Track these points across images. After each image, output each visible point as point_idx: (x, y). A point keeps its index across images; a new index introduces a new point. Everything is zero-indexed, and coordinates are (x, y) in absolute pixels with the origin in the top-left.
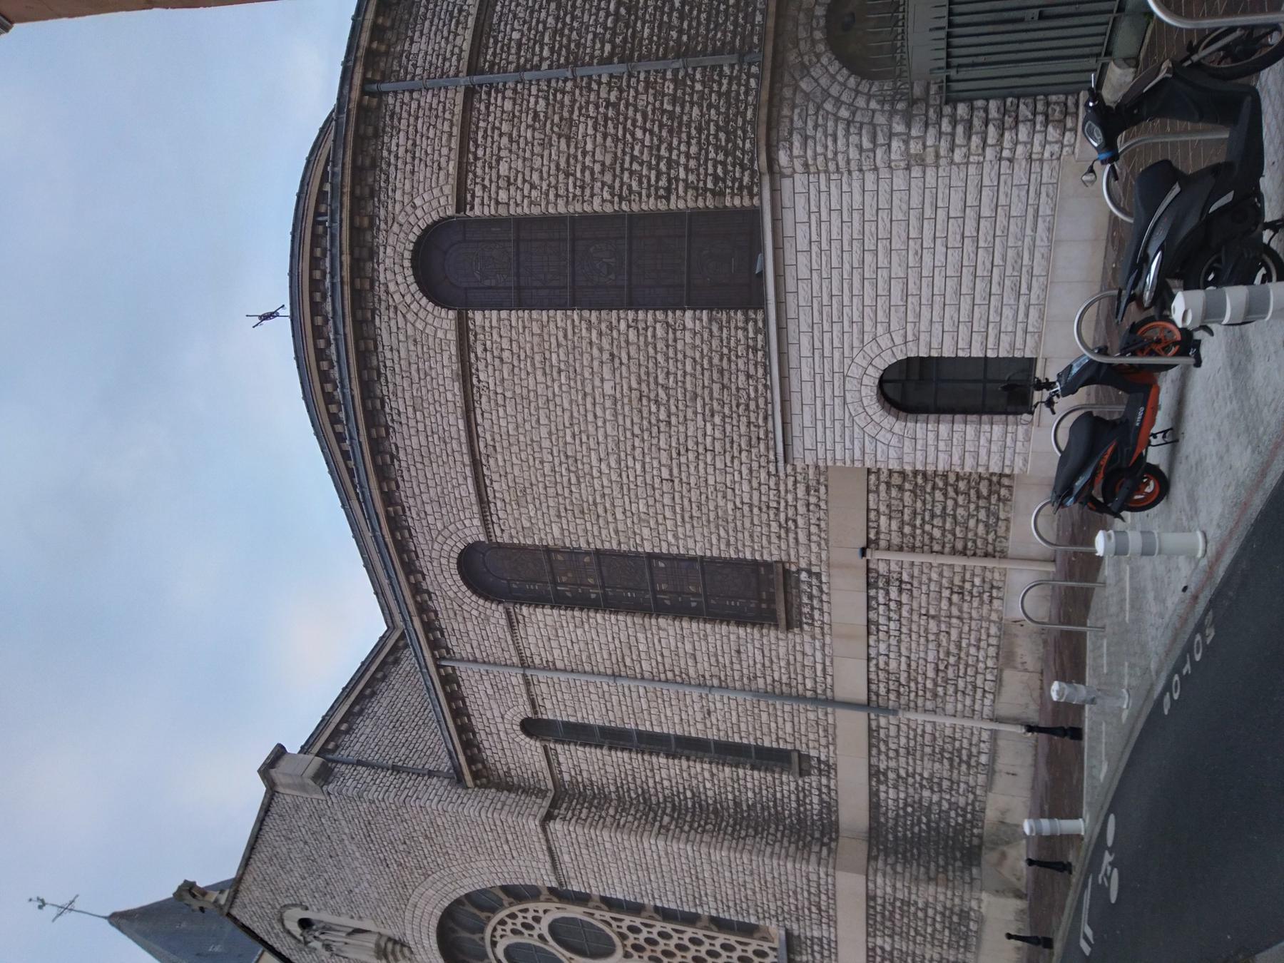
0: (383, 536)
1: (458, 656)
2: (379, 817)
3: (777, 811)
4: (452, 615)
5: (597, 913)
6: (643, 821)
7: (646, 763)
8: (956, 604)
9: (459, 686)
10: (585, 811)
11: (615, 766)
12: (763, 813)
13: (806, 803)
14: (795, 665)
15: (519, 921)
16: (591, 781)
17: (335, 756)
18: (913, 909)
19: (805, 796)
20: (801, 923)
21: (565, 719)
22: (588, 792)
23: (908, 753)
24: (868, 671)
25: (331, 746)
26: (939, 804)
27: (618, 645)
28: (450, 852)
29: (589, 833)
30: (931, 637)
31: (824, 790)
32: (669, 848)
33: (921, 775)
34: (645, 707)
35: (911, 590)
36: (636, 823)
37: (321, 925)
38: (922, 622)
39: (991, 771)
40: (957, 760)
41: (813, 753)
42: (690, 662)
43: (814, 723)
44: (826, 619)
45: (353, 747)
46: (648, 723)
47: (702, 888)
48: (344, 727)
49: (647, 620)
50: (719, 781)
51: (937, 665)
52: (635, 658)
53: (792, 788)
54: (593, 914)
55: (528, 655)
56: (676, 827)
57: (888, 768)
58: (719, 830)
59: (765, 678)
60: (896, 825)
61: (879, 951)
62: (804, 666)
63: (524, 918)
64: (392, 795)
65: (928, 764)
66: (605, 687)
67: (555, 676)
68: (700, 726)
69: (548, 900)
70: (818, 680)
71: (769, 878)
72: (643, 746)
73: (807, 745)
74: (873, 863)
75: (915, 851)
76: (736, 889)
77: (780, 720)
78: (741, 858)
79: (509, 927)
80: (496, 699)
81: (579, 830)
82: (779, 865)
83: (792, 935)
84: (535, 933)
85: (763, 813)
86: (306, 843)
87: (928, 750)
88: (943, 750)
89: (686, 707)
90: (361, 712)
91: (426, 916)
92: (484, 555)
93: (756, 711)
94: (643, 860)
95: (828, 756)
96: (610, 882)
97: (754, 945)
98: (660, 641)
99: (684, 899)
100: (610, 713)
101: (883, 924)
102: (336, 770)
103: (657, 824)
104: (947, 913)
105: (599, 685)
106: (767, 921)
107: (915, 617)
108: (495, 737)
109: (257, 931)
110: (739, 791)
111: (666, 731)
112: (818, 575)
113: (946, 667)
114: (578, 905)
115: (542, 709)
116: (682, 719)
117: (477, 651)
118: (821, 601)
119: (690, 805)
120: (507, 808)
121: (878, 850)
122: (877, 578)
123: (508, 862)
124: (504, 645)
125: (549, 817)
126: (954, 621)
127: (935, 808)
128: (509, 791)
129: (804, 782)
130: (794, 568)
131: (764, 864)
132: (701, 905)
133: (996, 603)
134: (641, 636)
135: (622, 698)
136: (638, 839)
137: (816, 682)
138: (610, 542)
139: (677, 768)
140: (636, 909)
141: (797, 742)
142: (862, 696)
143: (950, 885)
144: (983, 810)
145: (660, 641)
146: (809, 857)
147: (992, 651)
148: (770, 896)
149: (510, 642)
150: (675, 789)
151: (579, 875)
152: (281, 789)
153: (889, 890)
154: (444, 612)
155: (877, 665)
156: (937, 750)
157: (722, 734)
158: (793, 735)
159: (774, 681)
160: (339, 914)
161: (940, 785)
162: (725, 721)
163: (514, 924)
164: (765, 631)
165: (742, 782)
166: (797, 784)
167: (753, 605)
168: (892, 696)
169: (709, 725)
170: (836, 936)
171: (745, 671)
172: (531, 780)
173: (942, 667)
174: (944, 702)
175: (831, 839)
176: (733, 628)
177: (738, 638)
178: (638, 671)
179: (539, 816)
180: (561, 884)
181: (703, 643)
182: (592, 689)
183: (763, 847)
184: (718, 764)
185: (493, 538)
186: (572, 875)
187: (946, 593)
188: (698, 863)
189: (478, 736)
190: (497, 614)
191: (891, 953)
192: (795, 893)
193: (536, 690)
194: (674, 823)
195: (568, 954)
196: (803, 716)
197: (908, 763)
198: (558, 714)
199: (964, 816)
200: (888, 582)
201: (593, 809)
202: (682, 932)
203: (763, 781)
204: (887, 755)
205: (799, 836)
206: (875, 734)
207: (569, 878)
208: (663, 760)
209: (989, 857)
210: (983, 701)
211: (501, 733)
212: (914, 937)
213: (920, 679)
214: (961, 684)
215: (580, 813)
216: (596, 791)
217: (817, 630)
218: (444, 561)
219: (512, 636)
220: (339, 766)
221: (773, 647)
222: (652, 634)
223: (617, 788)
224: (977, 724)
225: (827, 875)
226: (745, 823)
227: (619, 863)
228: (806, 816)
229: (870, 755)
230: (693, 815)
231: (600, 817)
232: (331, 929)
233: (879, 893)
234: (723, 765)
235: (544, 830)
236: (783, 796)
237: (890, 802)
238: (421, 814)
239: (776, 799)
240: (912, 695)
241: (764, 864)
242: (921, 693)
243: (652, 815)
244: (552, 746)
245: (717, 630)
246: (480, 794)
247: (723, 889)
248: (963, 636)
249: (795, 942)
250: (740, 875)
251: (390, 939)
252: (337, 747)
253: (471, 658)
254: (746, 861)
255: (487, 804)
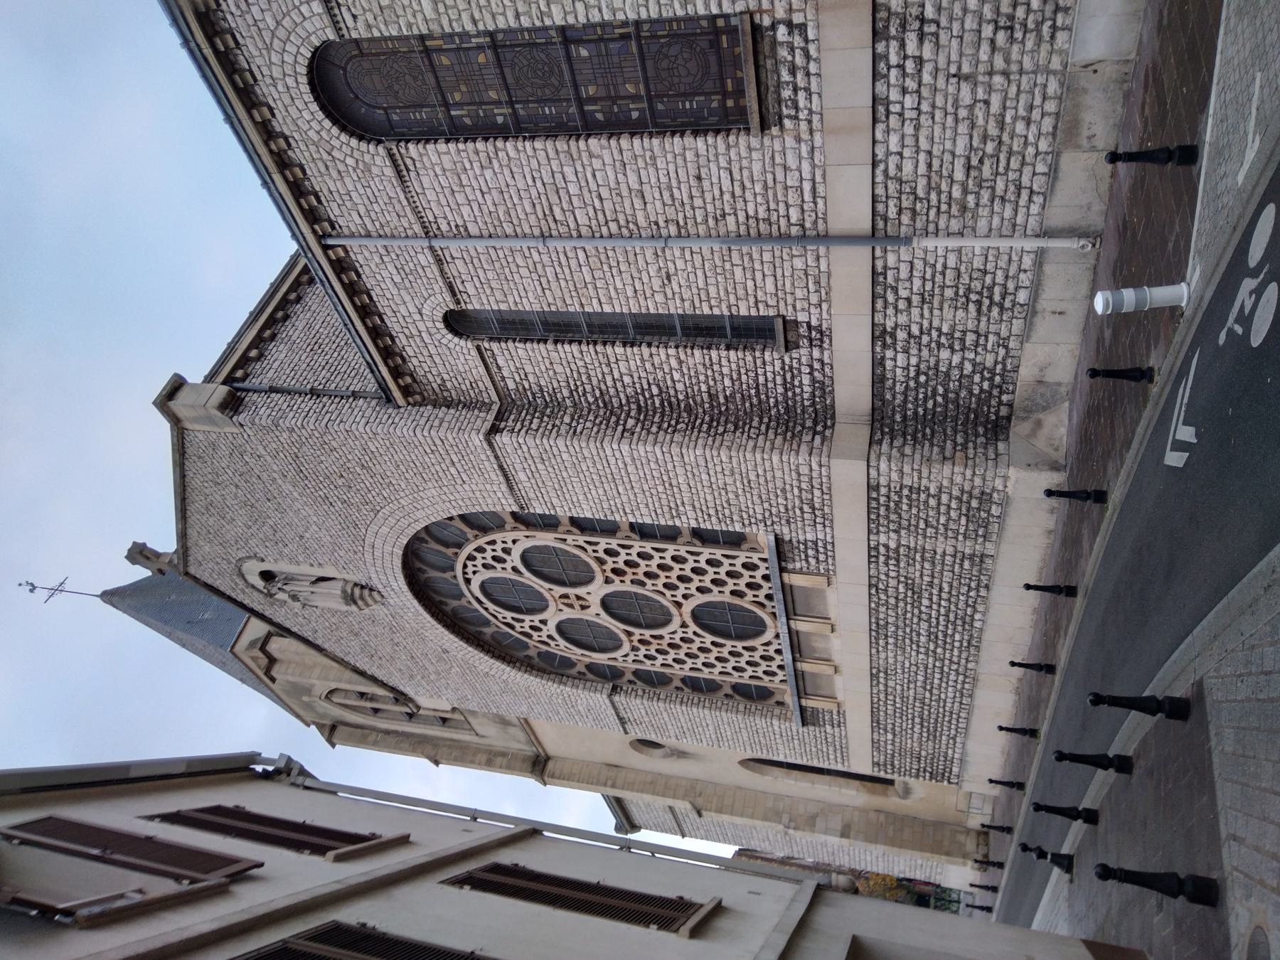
0: (198, 45)
1: (346, 231)
2: (305, 449)
3: (760, 401)
4: (323, 169)
5: (569, 538)
6: (603, 426)
7: (600, 355)
8: (1001, 49)
9: (359, 275)
10: (535, 421)
11: (564, 363)
12: (743, 404)
13: (794, 386)
14: (774, 188)
15: (489, 554)
16: (540, 386)
17: (246, 384)
18: (923, 496)
19: (793, 377)
20: (793, 526)
21: (495, 307)
22: (539, 401)
23: (923, 301)
24: (874, 183)
25: (239, 374)
26: (961, 366)
27: (542, 190)
28: (394, 482)
29: (542, 444)
30: (963, 113)
31: (817, 366)
32: (635, 452)
33: (939, 330)
34: (588, 279)
35: (936, 35)
36: (595, 429)
37: (284, 576)
38: (951, 89)
39: (1031, 311)
40: (986, 302)
41: (802, 317)
42: (638, 204)
43: (801, 274)
44: (815, 106)
45: (264, 375)
46: (595, 301)
47: (677, 496)
48: (253, 353)
49: (573, 143)
50: (689, 369)
51: (968, 159)
52: (565, 206)
53: (777, 369)
54: (565, 540)
55: (432, 219)
56: (642, 429)
57: (896, 325)
58: (693, 428)
59: (736, 215)
60: (905, 401)
61: (882, 550)
62: (786, 188)
63: (494, 550)
64: (312, 420)
65: (948, 313)
66: (536, 257)
67: (470, 244)
68: (659, 298)
69: (514, 529)
70: (806, 207)
71: (753, 477)
72: (595, 336)
73: (794, 307)
74: (875, 447)
75: (928, 431)
76: (716, 494)
77: (759, 276)
78: (719, 455)
79: (479, 562)
80: (406, 289)
81: (530, 440)
82: (763, 459)
83: (783, 540)
84: (508, 566)
85: (743, 404)
86: (237, 486)
87: (949, 293)
88: (969, 290)
89: (640, 272)
90: (273, 337)
91: (387, 557)
92: (345, 70)
93: (728, 266)
94: (608, 470)
95: (820, 320)
96: (575, 499)
97: (742, 557)
98: (594, 176)
99: (659, 511)
100: (547, 292)
101: (887, 517)
102: (247, 399)
103: (620, 428)
104: (965, 497)
105: (527, 255)
106: (754, 527)
107: (941, 83)
108: (418, 340)
109: (222, 589)
110: (714, 379)
111: (618, 310)
112: (802, 28)
113: (981, 161)
114: (547, 531)
115: (465, 296)
116: (636, 291)
117: (367, 220)
118: (808, 74)
119: (657, 403)
120: (445, 425)
121: (883, 434)
122: (888, 20)
123: (459, 488)
124: (398, 207)
125: (494, 430)
126: (998, 80)
127: (955, 373)
128: (448, 407)
129: (791, 359)
130: (767, 21)
131: (746, 461)
132: (679, 516)
133: (1061, 36)
134: (568, 170)
135: (558, 270)
136: (599, 446)
137: (803, 211)
138: (504, 14)
139: (637, 358)
140: (610, 529)
141: (782, 304)
142: (865, 225)
143: (970, 463)
144: (1016, 369)
145: (594, 176)
146: (799, 446)
147: (1047, 124)
148: (755, 498)
149: (405, 203)
150: (638, 386)
151: (539, 495)
152: (187, 425)
153: (895, 476)
154: (312, 165)
155: (886, 172)
156: (961, 292)
157: (687, 304)
158: (776, 295)
159: (747, 217)
160: (298, 563)
161: (962, 340)
162: (689, 287)
163: (483, 558)
164: (732, 138)
165: (716, 367)
166: (783, 362)
167: (715, 105)
168: (905, 219)
169: (670, 295)
170: (833, 537)
171: (710, 208)
172: (471, 392)
173: (974, 162)
174: (975, 217)
175: (825, 427)
176: (689, 140)
177: (697, 155)
178: (572, 225)
179: (483, 430)
180: (522, 508)
181: (651, 170)
182: (520, 261)
183: (744, 442)
184: (686, 347)
185: (345, 31)
186: (532, 495)
187: (988, 31)
188: (670, 466)
189: (397, 340)
190: (378, 160)
191: (897, 550)
192: (784, 491)
193: (451, 270)
194: (640, 425)
195: (548, 586)
196: (787, 265)
197: (922, 316)
198: (485, 302)
199: (991, 379)
200: (903, 27)
201: (546, 419)
202: (663, 550)
203: (741, 363)
204: (896, 308)
205: (787, 427)
206: (881, 279)
207: (529, 500)
208: (619, 350)
209: (1019, 429)
210: (1028, 208)
211: (423, 334)
212: (925, 530)
213: (944, 187)
214: (1000, 185)
215: (531, 423)
216: (548, 399)
217: (804, 126)
218: (290, 81)
219: (404, 192)
220: (250, 394)
221: (745, 163)
222: (583, 166)
223: (571, 392)
224: (1018, 243)
225: (821, 466)
226: (723, 419)
227: (581, 476)
228: (795, 402)
229: (874, 310)
230: (663, 415)
231: (554, 426)
232: (293, 579)
233: (883, 481)
234: (692, 348)
235: (491, 445)
236: (766, 380)
237: (899, 371)
238: (350, 441)
239: (758, 385)
240: (933, 212)
241: (746, 461)
242: (944, 207)
243: (613, 419)
244: (486, 345)
245: (667, 146)
246: (414, 413)
247: (702, 495)
248: (1008, 103)
249: (787, 548)
250: (720, 476)
251: (356, 585)
252: (246, 376)
253: (363, 233)
254: (724, 459)
255: (422, 422)
